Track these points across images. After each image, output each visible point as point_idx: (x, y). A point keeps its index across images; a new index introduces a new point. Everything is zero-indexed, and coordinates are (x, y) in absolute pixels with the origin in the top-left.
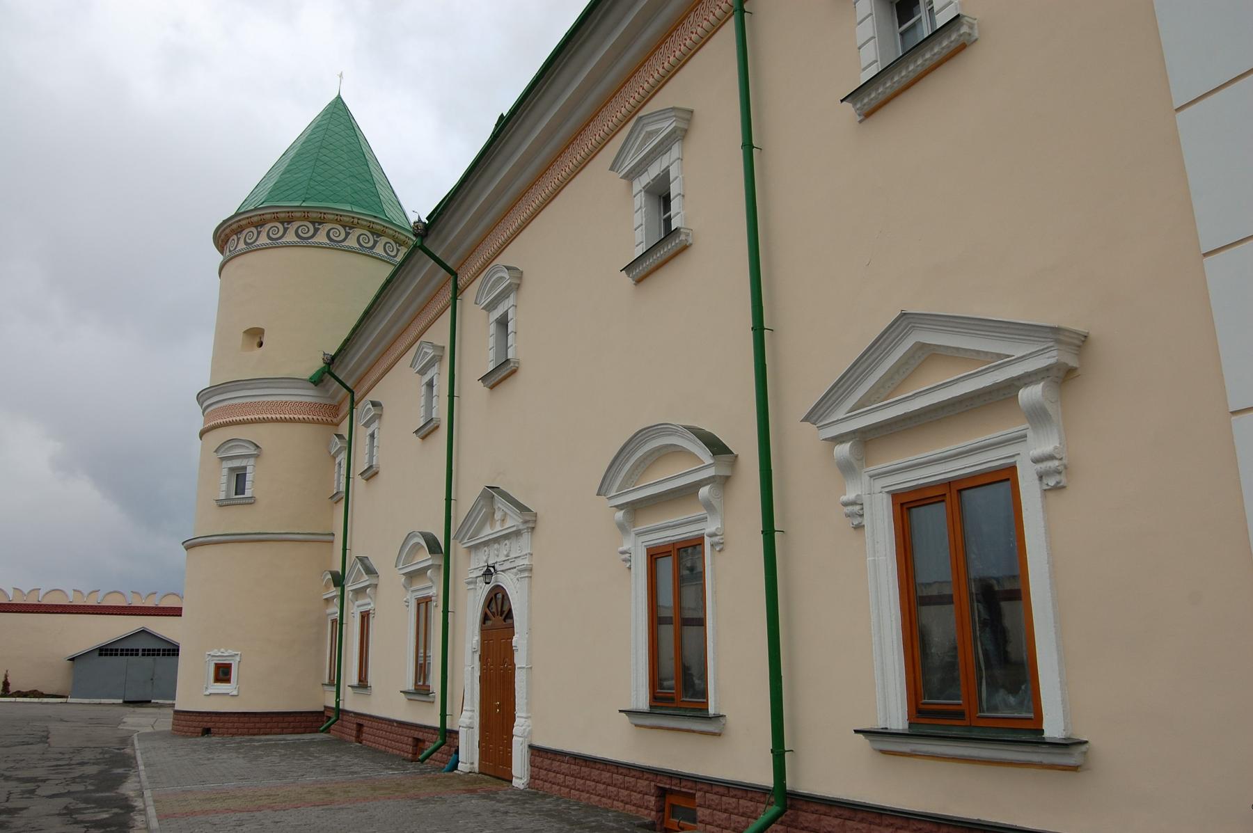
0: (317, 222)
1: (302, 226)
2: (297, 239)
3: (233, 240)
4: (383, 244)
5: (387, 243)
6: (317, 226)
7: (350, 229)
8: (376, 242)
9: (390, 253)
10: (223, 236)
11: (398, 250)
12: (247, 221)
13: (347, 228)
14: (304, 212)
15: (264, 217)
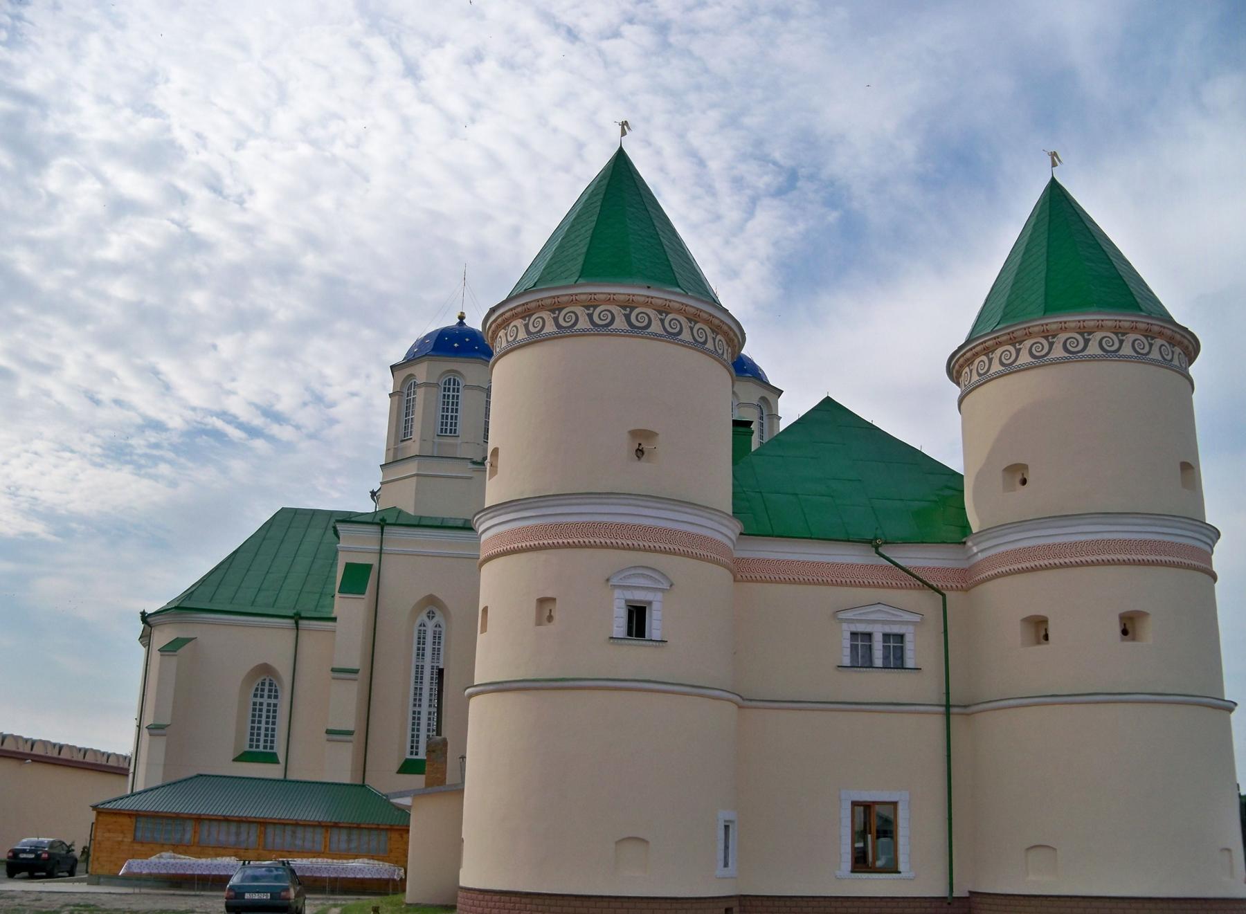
0: (1017, 342)
1: (1072, 338)
2: (1101, 352)
3: (966, 373)
4: (1159, 345)
5: (1162, 345)
6: (1086, 337)
7: (1122, 336)
8: (1151, 345)
9: (1165, 356)
10: (957, 366)
11: (1173, 352)
12: (982, 346)
13: (1120, 335)
14: (1025, 329)
15: (987, 344)
